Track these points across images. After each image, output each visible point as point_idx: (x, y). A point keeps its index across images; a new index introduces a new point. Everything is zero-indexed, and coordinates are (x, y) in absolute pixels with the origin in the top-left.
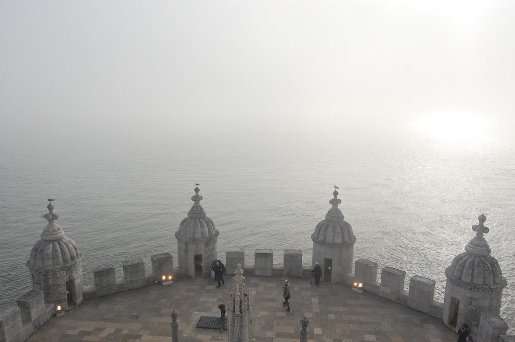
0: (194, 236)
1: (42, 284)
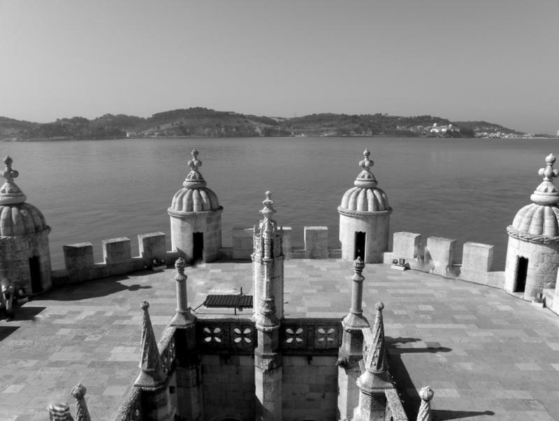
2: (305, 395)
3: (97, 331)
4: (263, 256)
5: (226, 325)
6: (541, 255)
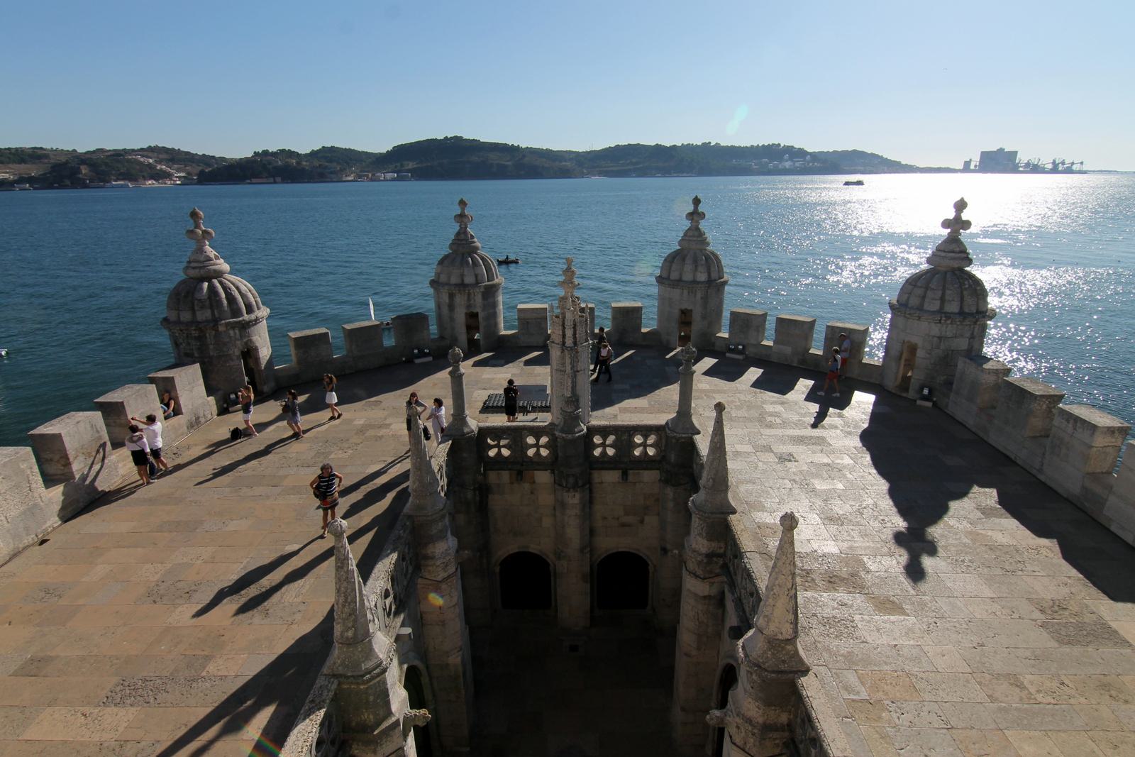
0: (463, 281)
1: (196, 355)
2: (618, 519)
3: (346, 445)
4: (564, 343)
5: (516, 435)
6: (935, 339)
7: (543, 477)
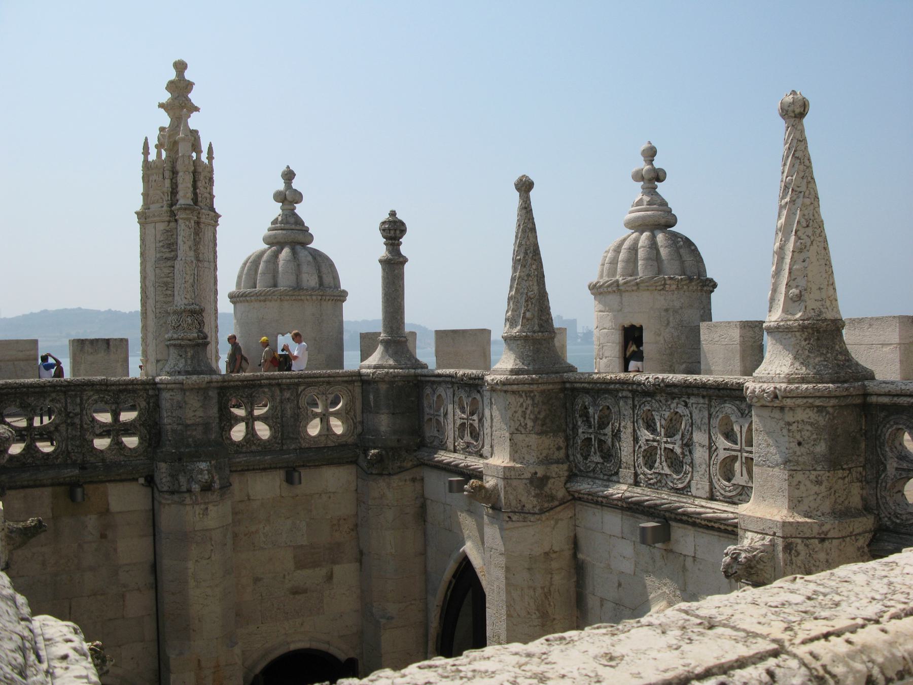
4: (173, 203)
6: (663, 314)
7: (125, 498)
